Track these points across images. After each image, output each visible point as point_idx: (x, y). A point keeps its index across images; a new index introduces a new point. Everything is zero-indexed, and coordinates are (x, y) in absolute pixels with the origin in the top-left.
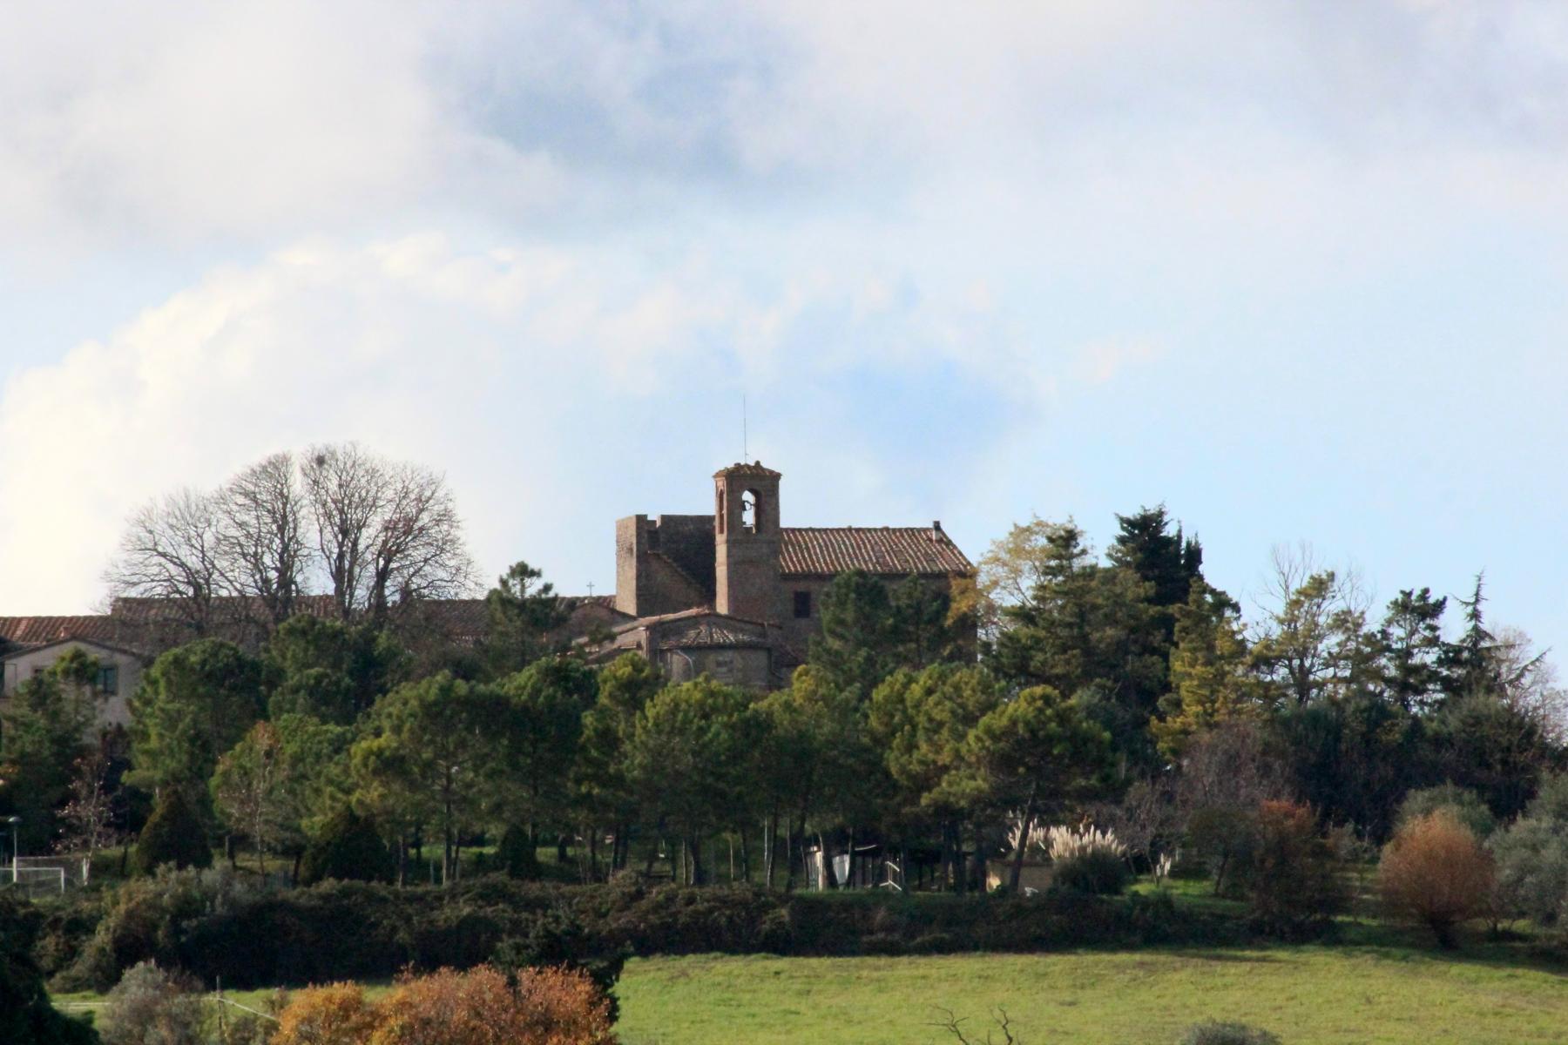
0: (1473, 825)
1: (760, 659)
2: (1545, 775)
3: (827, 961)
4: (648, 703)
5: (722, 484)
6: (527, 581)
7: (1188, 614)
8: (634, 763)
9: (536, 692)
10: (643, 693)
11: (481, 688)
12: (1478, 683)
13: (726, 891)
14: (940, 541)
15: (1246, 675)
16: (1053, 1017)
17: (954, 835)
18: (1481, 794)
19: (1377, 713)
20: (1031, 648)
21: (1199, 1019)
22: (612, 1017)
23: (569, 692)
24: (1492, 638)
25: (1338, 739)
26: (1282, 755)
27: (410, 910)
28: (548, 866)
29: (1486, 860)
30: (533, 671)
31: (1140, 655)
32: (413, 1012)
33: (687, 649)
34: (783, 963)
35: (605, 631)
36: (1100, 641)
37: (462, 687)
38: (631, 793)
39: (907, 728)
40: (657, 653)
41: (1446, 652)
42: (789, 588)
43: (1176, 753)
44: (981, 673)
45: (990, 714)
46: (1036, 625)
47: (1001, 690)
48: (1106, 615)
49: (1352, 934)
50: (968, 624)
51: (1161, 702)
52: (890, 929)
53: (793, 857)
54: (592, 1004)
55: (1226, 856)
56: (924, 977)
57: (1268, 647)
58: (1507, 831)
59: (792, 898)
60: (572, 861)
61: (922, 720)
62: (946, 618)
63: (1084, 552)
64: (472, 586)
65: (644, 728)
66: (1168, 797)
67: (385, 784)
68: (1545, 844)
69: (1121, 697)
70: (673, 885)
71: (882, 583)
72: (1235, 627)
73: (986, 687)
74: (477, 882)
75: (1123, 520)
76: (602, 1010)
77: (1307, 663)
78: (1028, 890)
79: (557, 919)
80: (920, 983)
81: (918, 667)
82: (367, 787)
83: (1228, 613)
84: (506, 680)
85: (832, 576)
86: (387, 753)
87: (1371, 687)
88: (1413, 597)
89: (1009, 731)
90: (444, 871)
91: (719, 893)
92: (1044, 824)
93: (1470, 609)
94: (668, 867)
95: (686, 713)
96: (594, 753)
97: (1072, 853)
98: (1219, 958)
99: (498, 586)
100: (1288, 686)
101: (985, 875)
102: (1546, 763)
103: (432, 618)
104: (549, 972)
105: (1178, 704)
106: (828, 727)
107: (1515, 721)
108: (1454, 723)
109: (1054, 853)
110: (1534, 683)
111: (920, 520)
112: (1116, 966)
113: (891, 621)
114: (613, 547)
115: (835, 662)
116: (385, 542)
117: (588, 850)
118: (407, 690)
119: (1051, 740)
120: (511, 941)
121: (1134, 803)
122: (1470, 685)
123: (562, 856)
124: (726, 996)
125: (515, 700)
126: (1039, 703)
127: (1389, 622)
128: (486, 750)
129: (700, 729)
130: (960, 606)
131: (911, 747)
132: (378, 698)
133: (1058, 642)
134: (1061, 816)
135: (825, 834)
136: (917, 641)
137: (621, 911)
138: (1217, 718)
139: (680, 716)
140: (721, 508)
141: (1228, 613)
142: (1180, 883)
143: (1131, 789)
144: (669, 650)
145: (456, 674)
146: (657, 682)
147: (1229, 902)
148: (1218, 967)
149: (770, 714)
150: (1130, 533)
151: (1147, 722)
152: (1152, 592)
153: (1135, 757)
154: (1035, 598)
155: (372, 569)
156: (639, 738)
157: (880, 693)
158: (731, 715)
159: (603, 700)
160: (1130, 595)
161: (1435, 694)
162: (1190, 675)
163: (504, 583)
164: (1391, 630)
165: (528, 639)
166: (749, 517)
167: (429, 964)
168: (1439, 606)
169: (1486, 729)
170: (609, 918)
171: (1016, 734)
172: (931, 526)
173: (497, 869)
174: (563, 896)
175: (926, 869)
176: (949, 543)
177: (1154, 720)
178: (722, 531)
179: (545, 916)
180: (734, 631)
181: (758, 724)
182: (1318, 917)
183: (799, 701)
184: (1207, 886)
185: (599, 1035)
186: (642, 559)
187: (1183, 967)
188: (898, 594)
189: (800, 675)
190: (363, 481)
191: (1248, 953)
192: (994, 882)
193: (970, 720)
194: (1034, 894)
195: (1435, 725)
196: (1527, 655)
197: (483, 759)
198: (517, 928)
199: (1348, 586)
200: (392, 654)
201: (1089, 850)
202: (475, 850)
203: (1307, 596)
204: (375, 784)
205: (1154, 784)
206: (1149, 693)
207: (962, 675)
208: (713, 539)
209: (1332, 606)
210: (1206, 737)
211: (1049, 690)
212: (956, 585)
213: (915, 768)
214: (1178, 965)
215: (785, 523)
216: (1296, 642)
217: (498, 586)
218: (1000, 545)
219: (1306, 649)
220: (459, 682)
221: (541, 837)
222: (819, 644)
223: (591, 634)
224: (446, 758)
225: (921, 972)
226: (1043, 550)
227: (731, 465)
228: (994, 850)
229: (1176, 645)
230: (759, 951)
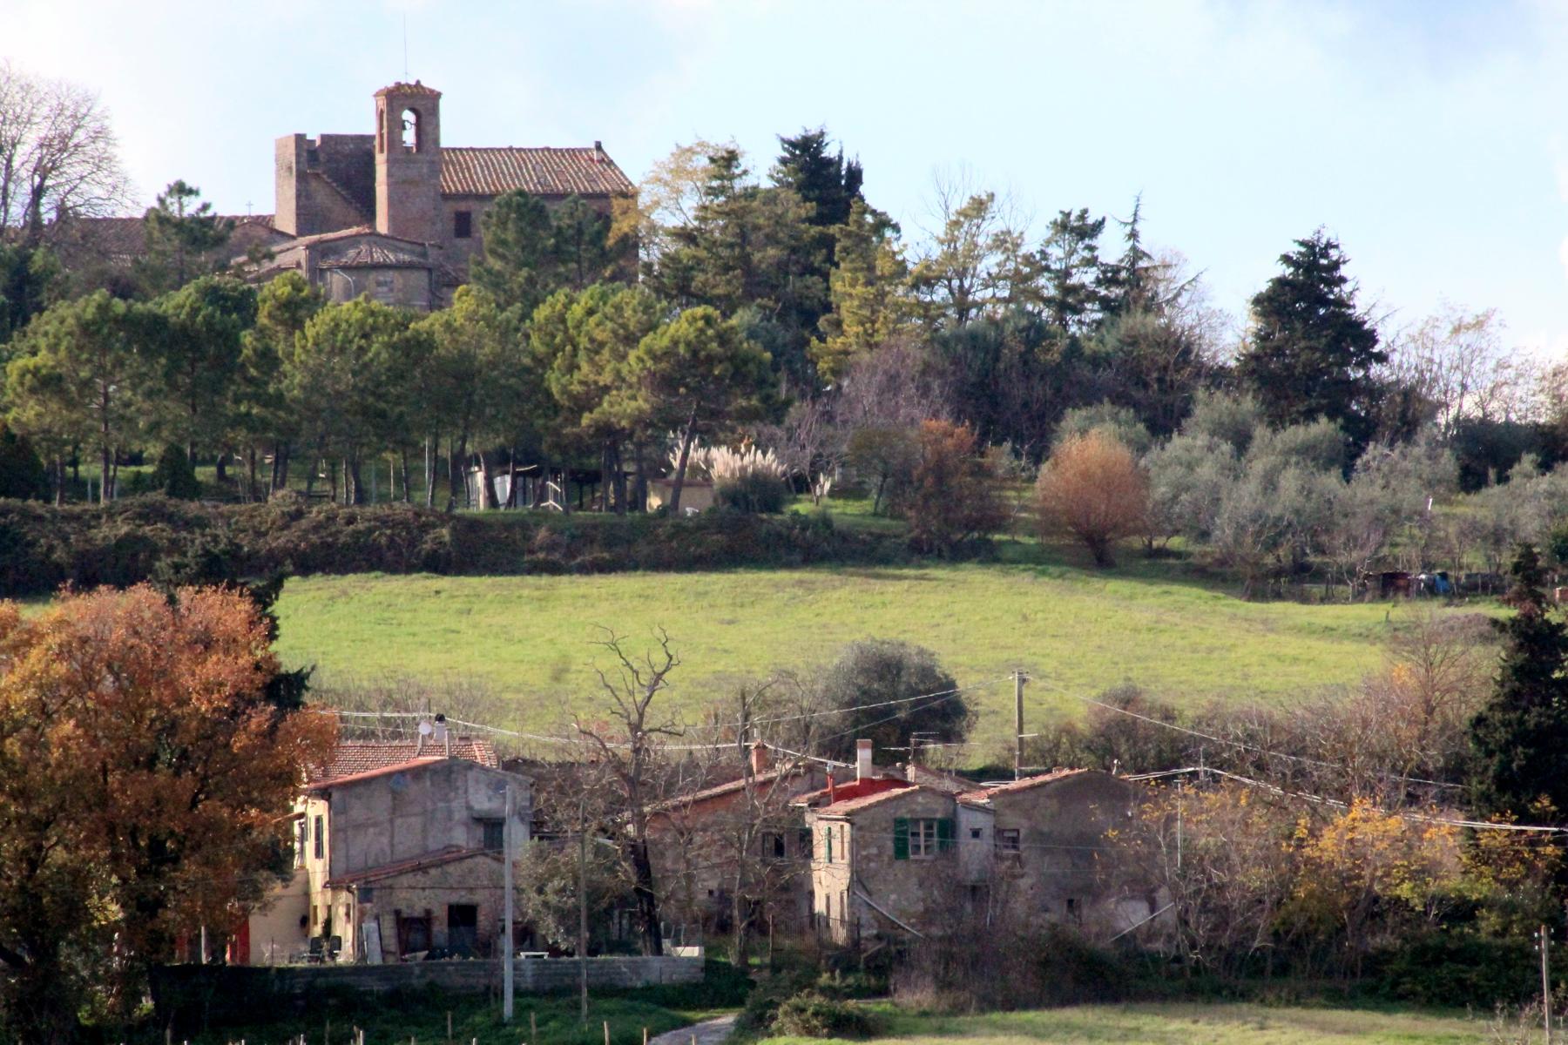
0: (1130, 442)
1: (420, 279)
2: (1201, 394)
3: (487, 580)
4: (308, 323)
5: (382, 103)
6: (185, 199)
7: (849, 235)
8: (293, 381)
9: (195, 311)
10: (302, 313)
11: (139, 307)
12: (1135, 303)
13: (387, 511)
14: (601, 161)
15: (906, 295)
16: (711, 635)
17: (615, 456)
18: (1137, 411)
19: (1036, 333)
20: (692, 268)
21: (859, 637)
22: (272, 636)
23: (226, 311)
24: (1149, 257)
25: (997, 359)
26: (942, 374)
27: (68, 529)
28: (207, 485)
29: (1143, 480)
30: (192, 290)
31: (802, 275)
32: (71, 630)
33: (346, 268)
34: (445, 582)
35: (264, 250)
36: (760, 262)
37: (120, 306)
38: (291, 412)
39: (569, 348)
40: (317, 273)
41: (1104, 272)
42: (449, 208)
43: (837, 373)
44: (642, 293)
45: (651, 334)
46: (697, 245)
47: (663, 310)
48: (767, 236)
49: (1009, 553)
50: (629, 245)
51: (822, 323)
52: (551, 547)
53: (453, 476)
54: (252, 623)
55: (885, 477)
56: (583, 597)
57: (928, 267)
58: (1163, 448)
59: (454, 517)
60: (231, 481)
61: (583, 342)
62: (607, 237)
63: (745, 172)
64: (129, 204)
65: (304, 347)
66: (829, 417)
67: (42, 403)
68: (1199, 461)
69: (781, 316)
70: (334, 505)
71: (542, 202)
72: (895, 247)
73: (647, 308)
74: (136, 500)
75: (783, 141)
76: (262, 629)
77: (967, 284)
78: (689, 511)
79: (215, 539)
80: (581, 602)
81: (579, 287)
82: (23, 406)
83: (888, 233)
84: (163, 299)
85: (492, 196)
86: (44, 371)
87: (1030, 307)
88: (1073, 218)
89: (668, 353)
90: (102, 490)
91: (379, 512)
92: (703, 444)
93: (1128, 229)
94: (328, 487)
95: (346, 332)
96: (253, 372)
97: (733, 474)
98: (878, 576)
99: (156, 205)
100: (946, 307)
101: (645, 496)
102: (1202, 382)
103: (85, 236)
104: (208, 590)
105: (838, 324)
106: (488, 348)
107: (1172, 341)
108: (1111, 342)
109: (714, 473)
110: (1191, 301)
111: (582, 140)
112: (776, 585)
113: (552, 241)
114: (272, 166)
115: (496, 282)
116: (41, 159)
117: (247, 470)
118: (64, 309)
119: (711, 360)
120: (169, 561)
121: (795, 424)
122: (1128, 305)
123: (221, 475)
124: (386, 615)
125: (174, 319)
126: (701, 324)
127: (1048, 242)
128: (144, 370)
129: (360, 348)
130: (621, 226)
131: (572, 367)
132: (34, 316)
133: (720, 262)
134: (721, 436)
135: (485, 454)
136: (578, 262)
137: (282, 529)
138: (877, 338)
139: (340, 336)
140: (381, 127)
141: (888, 233)
142: (840, 502)
143: (791, 409)
144: (329, 269)
145: (114, 293)
146: (316, 302)
147: (887, 521)
148: (877, 585)
149: (430, 334)
150: (792, 154)
151: (808, 342)
152: (813, 213)
153: (795, 378)
154: (697, 218)
155: (27, 187)
156: (300, 361)
157: (541, 313)
158: (391, 335)
159: (263, 319)
160: (791, 215)
161: (1093, 313)
162: (850, 295)
163: (161, 201)
164: (1049, 250)
165: (187, 258)
166: (409, 137)
167: (87, 582)
168: (1098, 226)
169: (1144, 349)
170: (268, 538)
171: (677, 354)
172: (593, 146)
173: (154, 488)
174: (221, 515)
175: (586, 488)
176: (611, 163)
177: (814, 341)
178: (382, 151)
179: (203, 535)
180: (396, 250)
181: (419, 343)
182: (976, 535)
183: (459, 320)
184: (867, 505)
185: (259, 654)
186: (302, 178)
187: (843, 585)
188: (559, 215)
189: (460, 296)
190: (18, 97)
191: (906, 572)
192: (654, 502)
193: (631, 340)
194: (696, 515)
195: (1093, 344)
196: (1182, 275)
197: (142, 377)
198: (175, 546)
199: (1007, 207)
200: (48, 272)
201: (750, 470)
202: (133, 469)
203: (966, 216)
204: (31, 403)
205: (814, 404)
206: (810, 314)
207: (623, 295)
208: (372, 158)
209: (990, 228)
210: (865, 357)
211: (710, 310)
212: (617, 204)
213: (576, 388)
214: (837, 584)
215: (445, 143)
216: (957, 264)
217: (156, 205)
218: (661, 165)
219: (965, 270)
220: (116, 300)
221: (199, 457)
222: (479, 264)
223: (250, 253)
224: (103, 376)
225: (582, 591)
226: (705, 170)
227: (391, 84)
228: (656, 470)
229: (837, 265)
230: (419, 570)
